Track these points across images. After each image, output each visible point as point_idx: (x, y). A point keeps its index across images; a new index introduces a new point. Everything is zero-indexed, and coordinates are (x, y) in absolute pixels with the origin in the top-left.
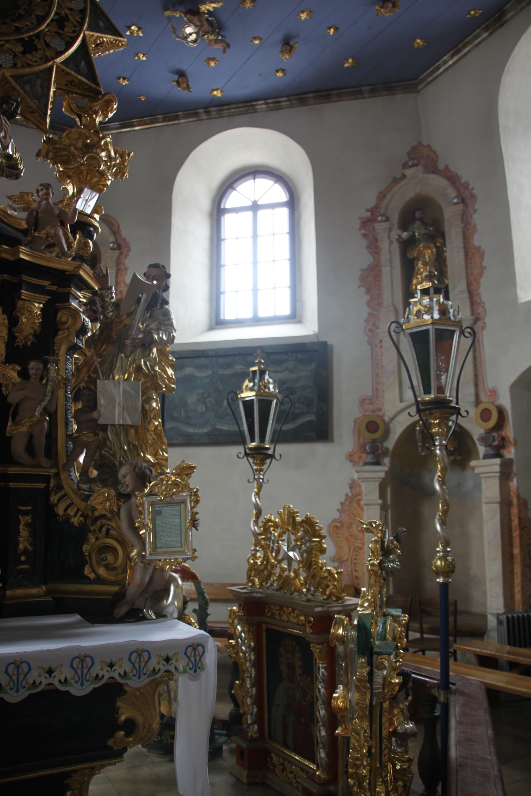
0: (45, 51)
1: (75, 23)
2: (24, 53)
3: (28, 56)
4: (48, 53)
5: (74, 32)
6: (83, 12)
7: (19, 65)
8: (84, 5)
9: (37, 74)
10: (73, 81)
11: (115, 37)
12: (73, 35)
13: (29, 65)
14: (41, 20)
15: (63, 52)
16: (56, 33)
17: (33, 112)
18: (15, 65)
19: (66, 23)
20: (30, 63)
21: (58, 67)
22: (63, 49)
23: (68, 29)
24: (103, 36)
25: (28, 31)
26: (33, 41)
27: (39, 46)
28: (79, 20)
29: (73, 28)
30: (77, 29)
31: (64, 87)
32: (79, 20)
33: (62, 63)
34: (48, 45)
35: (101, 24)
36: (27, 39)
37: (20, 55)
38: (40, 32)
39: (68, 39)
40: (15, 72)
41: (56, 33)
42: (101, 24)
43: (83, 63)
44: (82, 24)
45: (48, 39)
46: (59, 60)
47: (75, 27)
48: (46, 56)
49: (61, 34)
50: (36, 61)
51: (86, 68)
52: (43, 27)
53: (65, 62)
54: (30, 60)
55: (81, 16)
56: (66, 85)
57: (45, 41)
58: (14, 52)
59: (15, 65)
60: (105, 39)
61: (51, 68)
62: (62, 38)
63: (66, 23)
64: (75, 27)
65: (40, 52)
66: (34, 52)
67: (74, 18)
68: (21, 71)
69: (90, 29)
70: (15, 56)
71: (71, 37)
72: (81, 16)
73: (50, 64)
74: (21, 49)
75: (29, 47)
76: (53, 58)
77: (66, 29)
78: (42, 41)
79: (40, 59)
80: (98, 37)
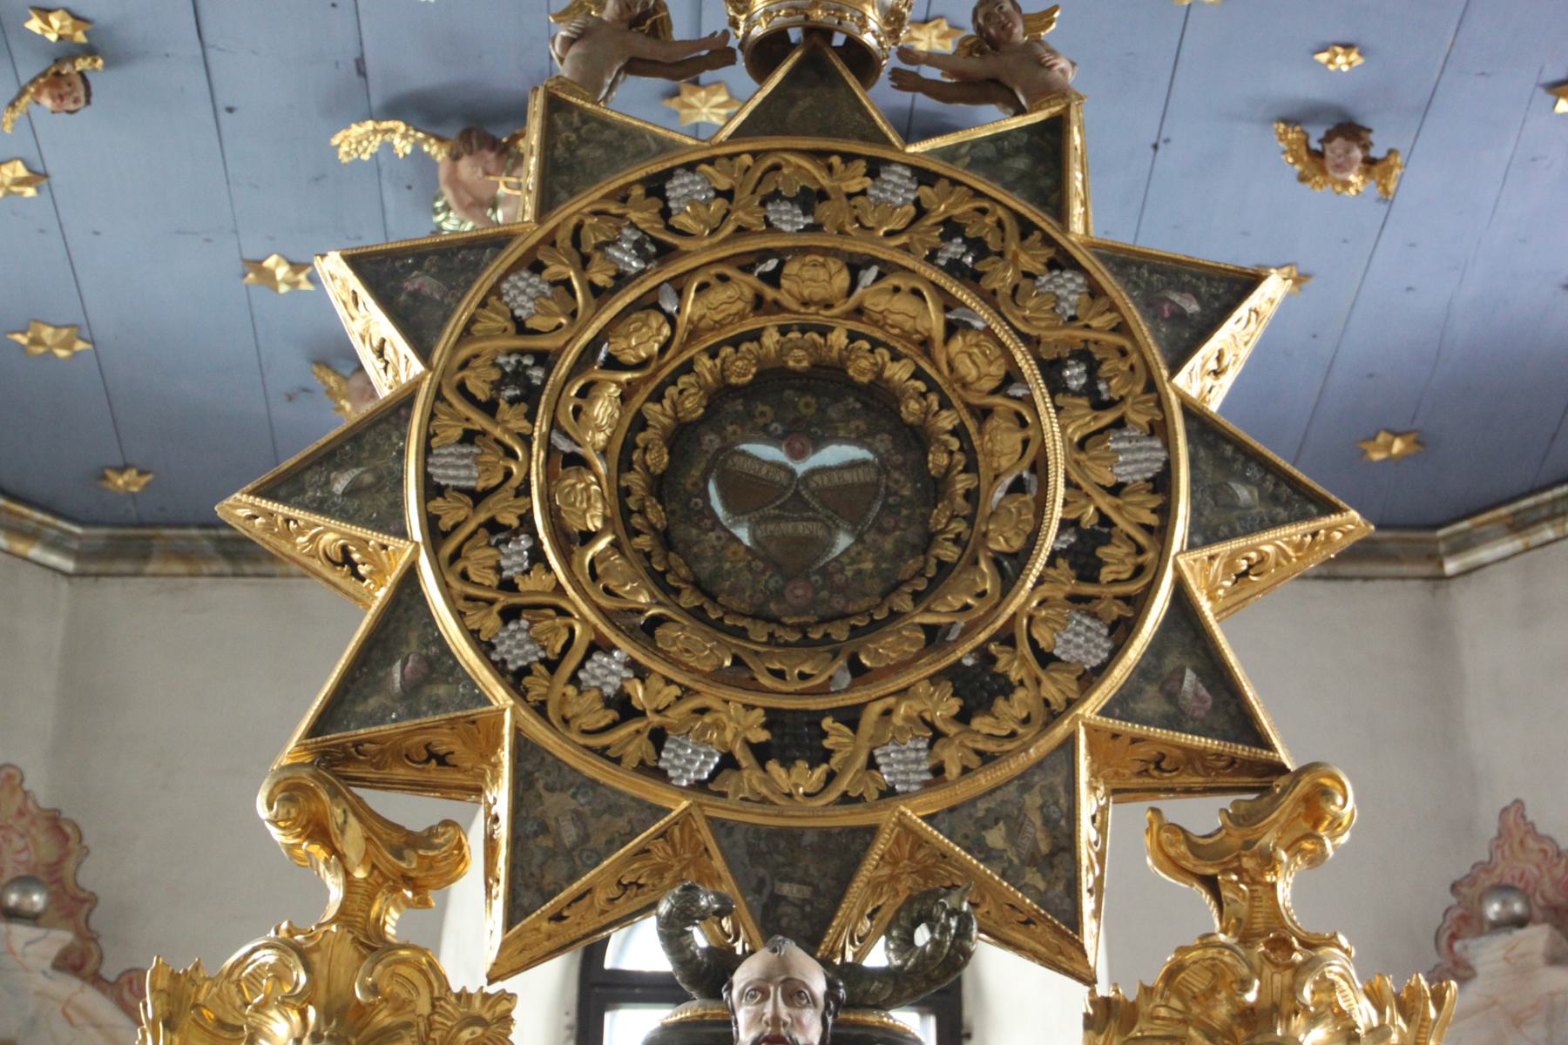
0: (1038, 682)
1: (1141, 538)
2: (963, 717)
3: (981, 724)
4: (1050, 691)
5: (1139, 571)
6: (1162, 483)
7: (953, 770)
8: (1162, 455)
9: (1024, 780)
10: (1163, 756)
11: (1305, 527)
12: (1134, 588)
13: (987, 758)
14: (1010, 567)
15: (1102, 670)
16: (1075, 599)
17: (1027, 922)
18: (938, 771)
19: (1102, 552)
20: (991, 747)
21: (1092, 731)
22: (1105, 655)
23: (1116, 560)
24: (1256, 539)
25: (968, 632)
26: (993, 660)
27: (1014, 676)
28: (1152, 520)
29: (1131, 562)
30: (1150, 556)
31: (1136, 782)
32: (1152, 520)
33: (1106, 712)
34: (1045, 658)
35: (1244, 494)
36: (969, 662)
37: (952, 729)
38: (1014, 615)
39: (1117, 610)
40: (939, 799)
41: (1075, 599)
42: (1244, 494)
43: (1190, 676)
44: (1160, 533)
45: (1043, 636)
46: (1089, 709)
47: (1140, 550)
48: (1047, 703)
49: (1088, 599)
50: (1013, 735)
51: (1204, 692)
52: (1023, 594)
53: (1117, 706)
54: (990, 736)
55: (1156, 501)
56: (1144, 772)
57: (1033, 643)
58: (930, 725)
59: (938, 771)
60: (1268, 548)
61: (1070, 742)
62: (1094, 616)
63: (1102, 552)
64: (1140, 550)
65: (1020, 694)
66: (1000, 703)
67: (1132, 515)
68: (961, 791)
69: (1204, 535)
70: (937, 735)
71: (1127, 599)
72: (1156, 501)
73: (1060, 731)
74: (955, 705)
75: (978, 688)
76: (1071, 704)
77: (1106, 574)
78: (1025, 648)
79: (1026, 721)
80: (1234, 555)
